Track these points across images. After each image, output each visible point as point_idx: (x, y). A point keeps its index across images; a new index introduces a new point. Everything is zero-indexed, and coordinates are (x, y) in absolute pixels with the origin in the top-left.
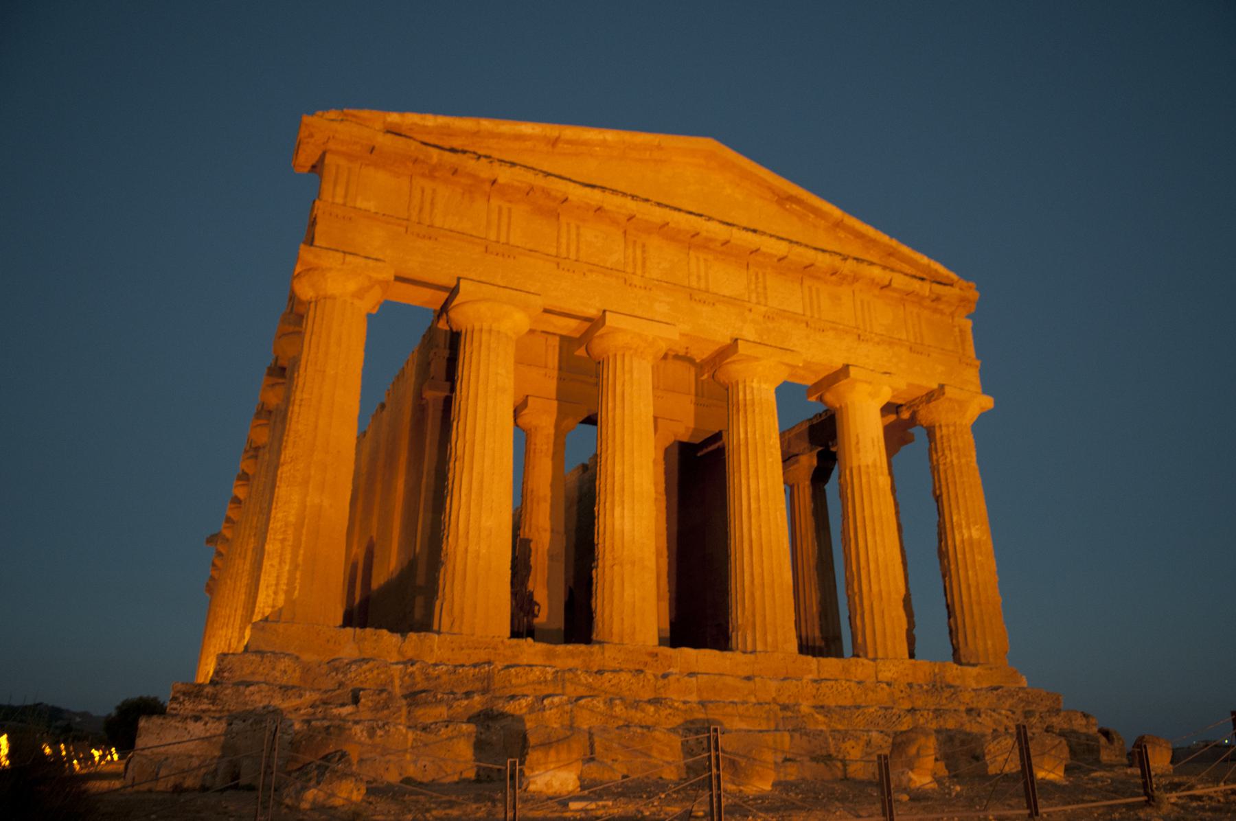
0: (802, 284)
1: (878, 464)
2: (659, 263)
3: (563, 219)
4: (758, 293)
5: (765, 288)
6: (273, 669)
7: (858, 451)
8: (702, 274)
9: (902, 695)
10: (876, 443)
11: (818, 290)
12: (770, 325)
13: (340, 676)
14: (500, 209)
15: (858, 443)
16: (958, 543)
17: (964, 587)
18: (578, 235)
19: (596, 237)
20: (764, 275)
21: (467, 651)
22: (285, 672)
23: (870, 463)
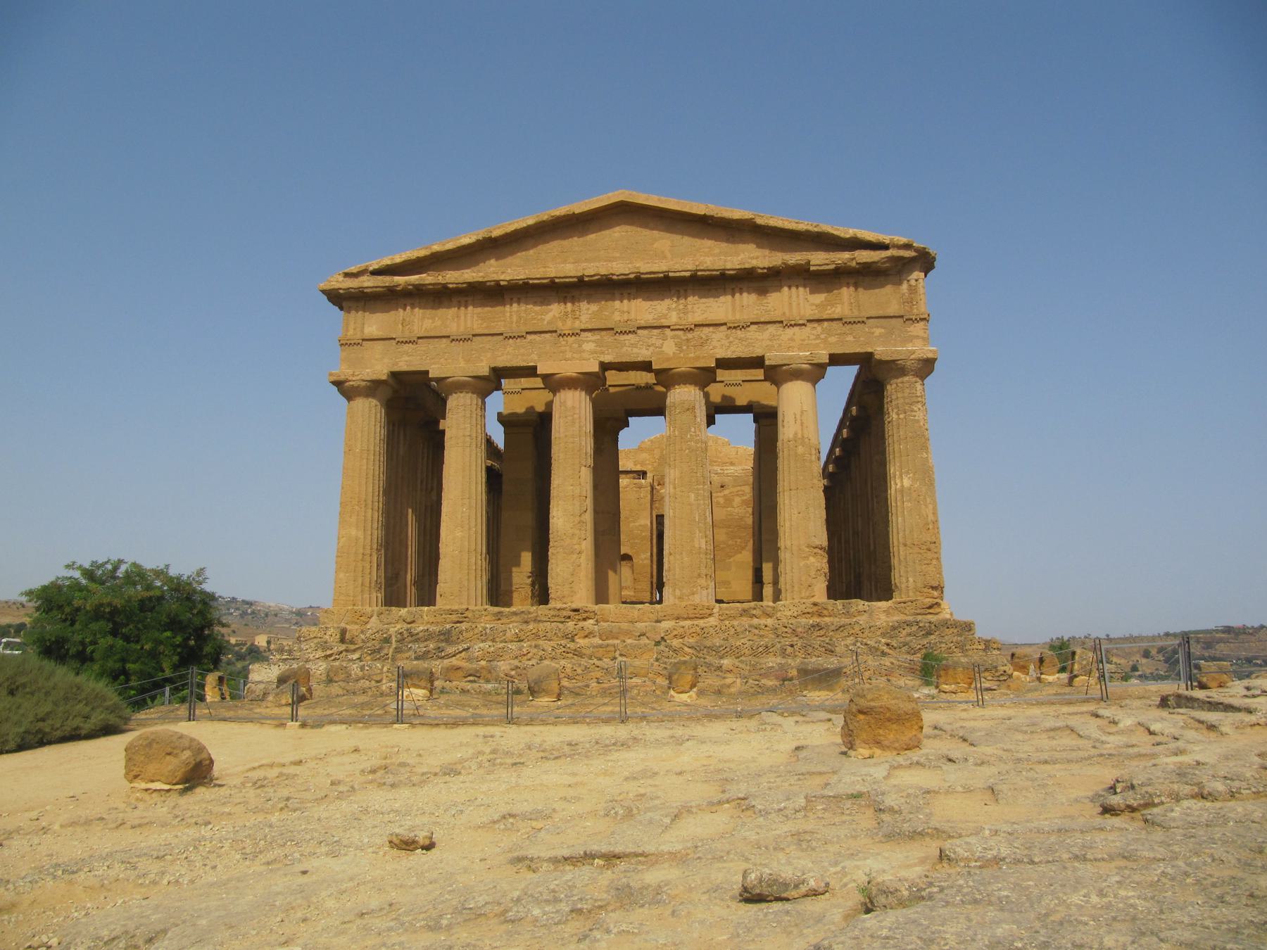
1: (800, 436)
2: (589, 309)
7: (783, 426)
9: (786, 630)
10: (798, 417)
12: (690, 335)
16: (893, 492)
17: (895, 530)
21: (444, 616)
23: (791, 436)
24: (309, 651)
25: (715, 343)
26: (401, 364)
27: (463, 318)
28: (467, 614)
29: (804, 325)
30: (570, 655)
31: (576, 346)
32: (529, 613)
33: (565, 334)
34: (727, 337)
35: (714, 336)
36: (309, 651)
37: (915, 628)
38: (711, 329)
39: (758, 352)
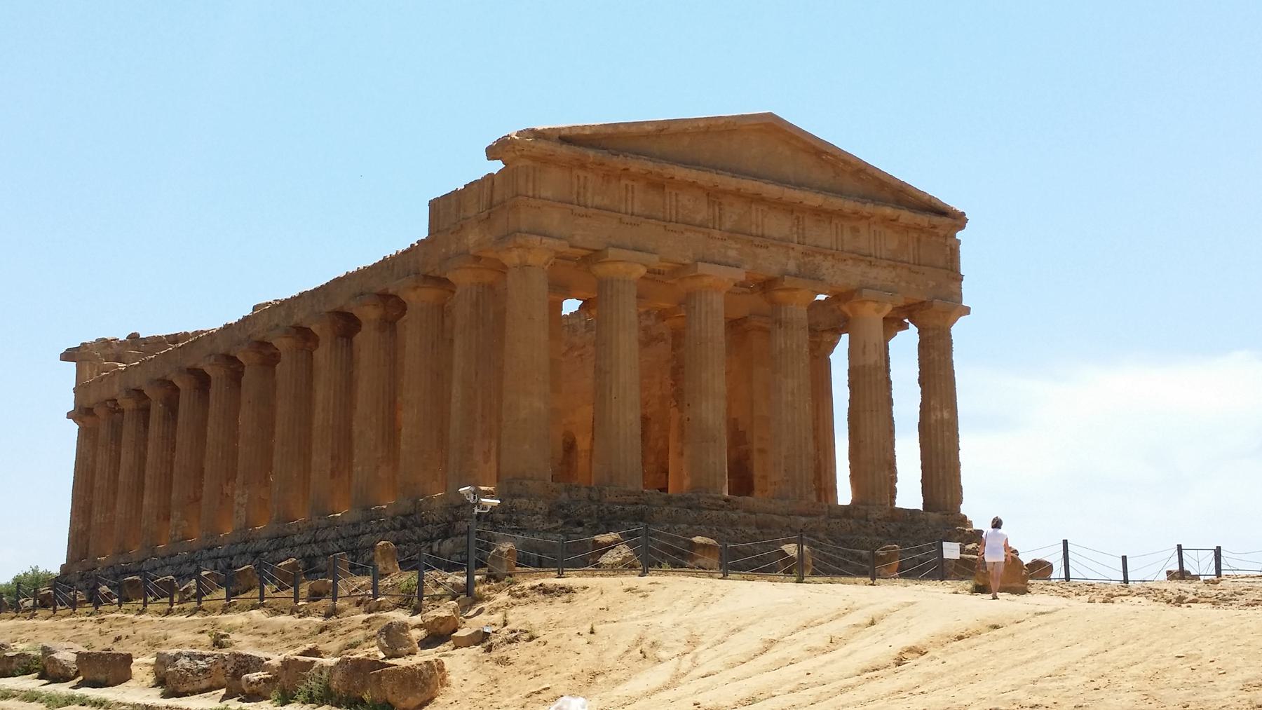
0: (831, 222)
3: (667, 190)
4: (798, 233)
5: (803, 229)
6: (535, 507)
7: (864, 353)
8: (760, 223)
11: (842, 225)
12: (806, 259)
13: (566, 511)
14: (626, 185)
15: (865, 347)
18: (677, 201)
19: (689, 200)
20: (803, 218)
22: (541, 508)
24: (537, 522)
25: (824, 271)
26: (578, 238)
27: (630, 203)
28: (642, 497)
29: (885, 268)
30: (747, 540)
31: (723, 250)
32: (693, 499)
33: (715, 238)
34: (833, 266)
35: (823, 263)
36: (537, 522)
37: (962, 535)
38: (822, 257)
39: (854, 283)
